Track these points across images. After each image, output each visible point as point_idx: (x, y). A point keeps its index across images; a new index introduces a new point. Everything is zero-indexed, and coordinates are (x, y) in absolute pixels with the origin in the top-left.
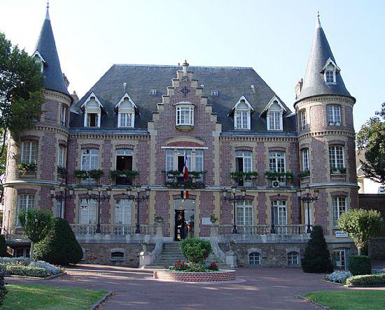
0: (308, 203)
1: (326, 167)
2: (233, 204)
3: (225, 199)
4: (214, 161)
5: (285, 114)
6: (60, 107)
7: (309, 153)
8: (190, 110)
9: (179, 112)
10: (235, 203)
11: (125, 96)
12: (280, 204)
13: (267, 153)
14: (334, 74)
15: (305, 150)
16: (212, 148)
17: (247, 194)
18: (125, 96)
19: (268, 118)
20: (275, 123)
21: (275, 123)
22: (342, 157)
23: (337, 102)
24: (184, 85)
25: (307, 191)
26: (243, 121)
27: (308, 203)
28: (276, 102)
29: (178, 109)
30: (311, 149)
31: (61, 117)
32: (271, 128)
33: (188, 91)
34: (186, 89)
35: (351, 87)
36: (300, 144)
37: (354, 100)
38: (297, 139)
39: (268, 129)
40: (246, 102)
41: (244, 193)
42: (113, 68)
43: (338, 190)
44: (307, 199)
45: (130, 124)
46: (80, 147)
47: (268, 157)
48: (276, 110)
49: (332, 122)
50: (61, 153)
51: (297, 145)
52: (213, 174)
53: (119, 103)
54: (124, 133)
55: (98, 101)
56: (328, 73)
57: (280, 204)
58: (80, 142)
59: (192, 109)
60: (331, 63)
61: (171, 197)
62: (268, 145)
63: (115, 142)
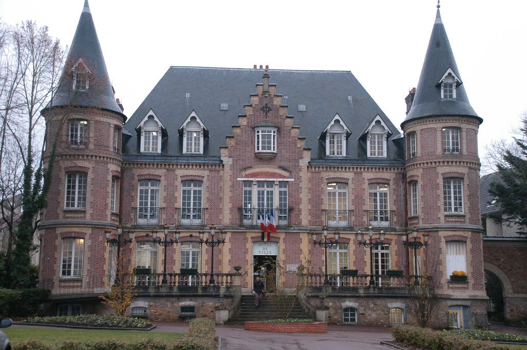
0: (415, 249)
1: (439, 204)
2: (324, 249)
3: (315, 243)
4: (301, 196)
5: (389, 135)
6: (112, 130)
7: (419, 187)
8: (272, 134)
9: (258, 136)
10: (326, 248)
11: (192, 115)
12: (268, 187)
13: (366, 185)
14: (454, 87)
15: (415, 183)
16: (299, 179)
17: (341, 236)
18: (192, 115)
19: (368, 143)
20: (378, 149)
21: (378, 149)
22: (460, 192)
23: (456, 124)
24: (265, 101)
25: (415, 234)
26: (338, 148)
27: (415, 249)
28: (378, 122)
29: (258, 132)
30: (420, 183)
31: (113, 141)
32: (371, 155)
33: (270, 110)
34: (266, 107)
35: (477, 103)
36: (409, 174)
37: (480, 121)
38: (405, 169)
39: (369, 155)
40: (342, 123)
41: (337, 236)
42: (172, 69)
43: (454, 233)
44: (416, 244)
45: (199, 149)
46: (136, 178)
47: (368, 190)
48: (378, 131)
49: (449, 150)
50: (113, 186)
51: (404, 176)
52: (300, 210)
53: (185, 124)
54: (192, 161)
55: (158, 121)
56: (446, 86)
57: (268, 187)
58: (137, 172)
59: (274, 132)
60: (450, 74)
61: (250, 240)
62: (368, 175)
63: (180, 172)
